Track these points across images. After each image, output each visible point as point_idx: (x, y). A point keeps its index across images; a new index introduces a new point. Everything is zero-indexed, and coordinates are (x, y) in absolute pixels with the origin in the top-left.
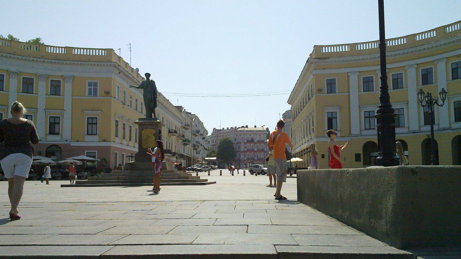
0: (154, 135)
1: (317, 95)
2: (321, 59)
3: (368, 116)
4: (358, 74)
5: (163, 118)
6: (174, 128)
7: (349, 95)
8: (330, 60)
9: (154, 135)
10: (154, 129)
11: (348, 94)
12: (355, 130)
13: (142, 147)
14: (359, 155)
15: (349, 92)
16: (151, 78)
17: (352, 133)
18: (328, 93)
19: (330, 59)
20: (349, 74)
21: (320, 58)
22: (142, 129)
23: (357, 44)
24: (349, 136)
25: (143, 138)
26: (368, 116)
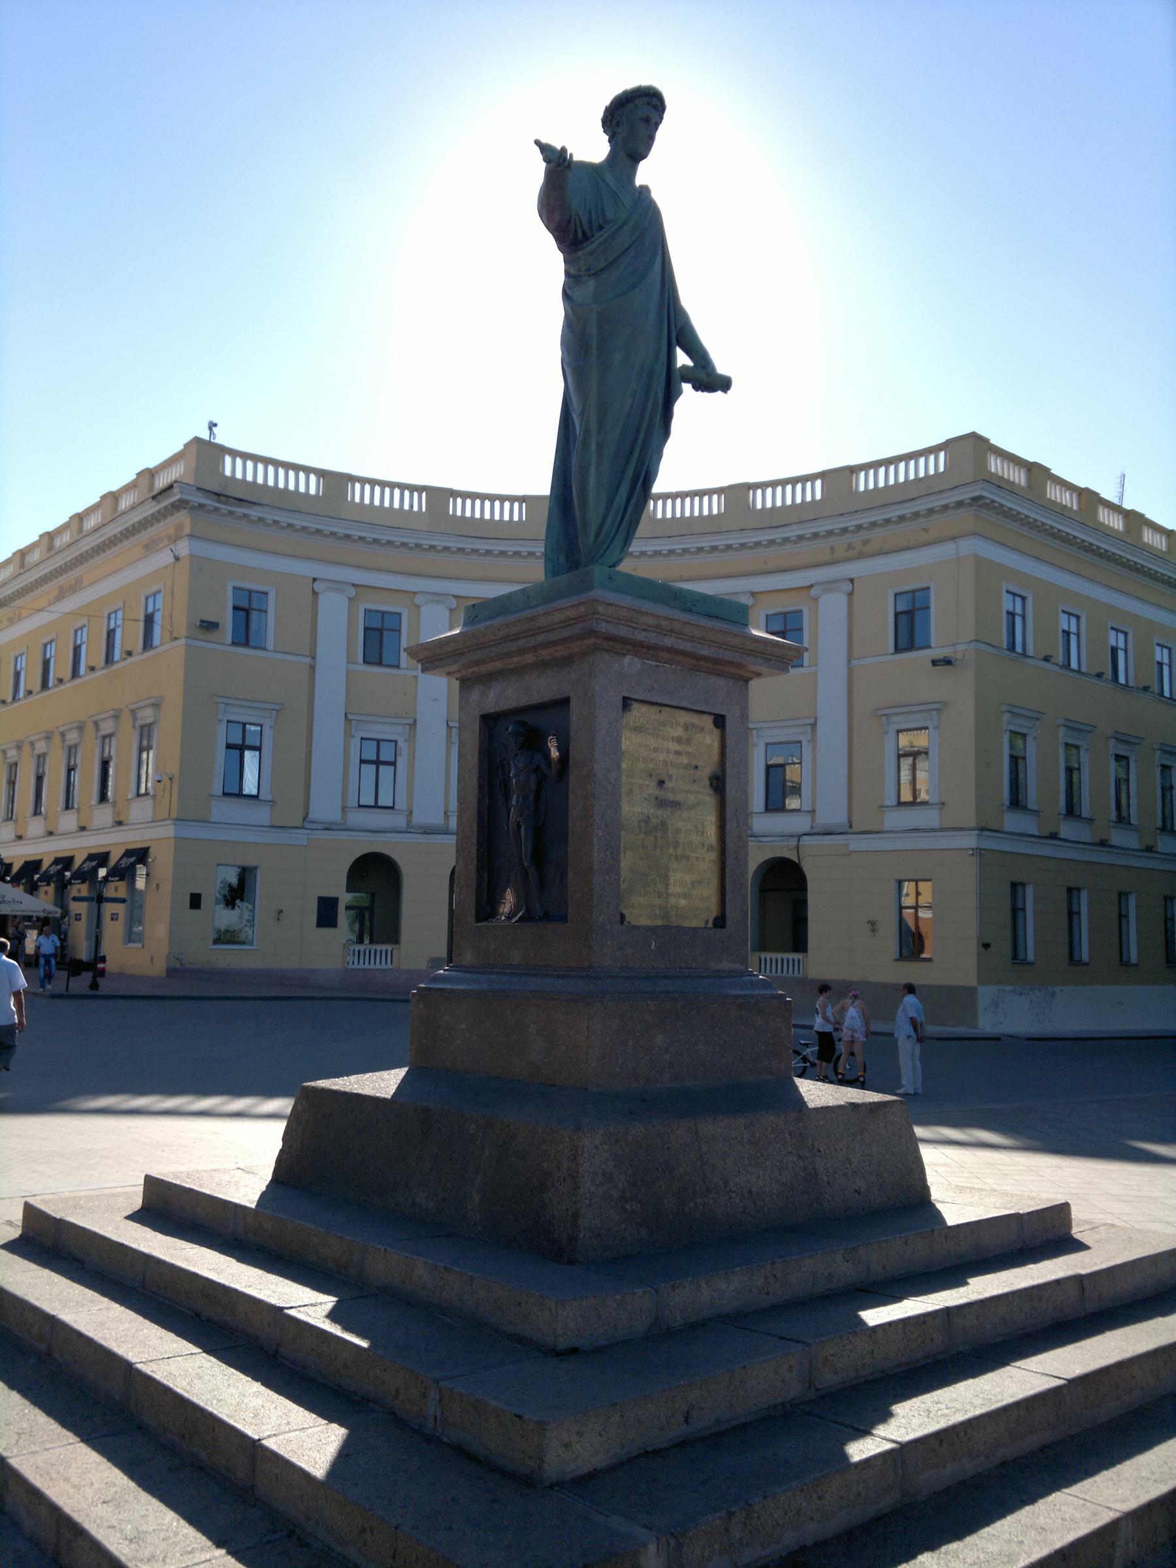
0: (718, 783)
1: (196, 643)
2: (222, 498)
3: (374, 758)
4: (352, 592)
7: (313, 668)
8: (254, 512)
10: (720, 721)
11: (308, 660)
12: (325, 807)
13: (623, 917)
14: (334, 901)
15: (314, 658)
16: (646, 174)
17: (311, 816)
18: (234, 644)
19: (257, 508)
20: (317, 587)
21: (218, 495)
22: (626, 703)
23: (352, 479)
24: (303, 828)
25: (626, 808)
26: (374, 758)
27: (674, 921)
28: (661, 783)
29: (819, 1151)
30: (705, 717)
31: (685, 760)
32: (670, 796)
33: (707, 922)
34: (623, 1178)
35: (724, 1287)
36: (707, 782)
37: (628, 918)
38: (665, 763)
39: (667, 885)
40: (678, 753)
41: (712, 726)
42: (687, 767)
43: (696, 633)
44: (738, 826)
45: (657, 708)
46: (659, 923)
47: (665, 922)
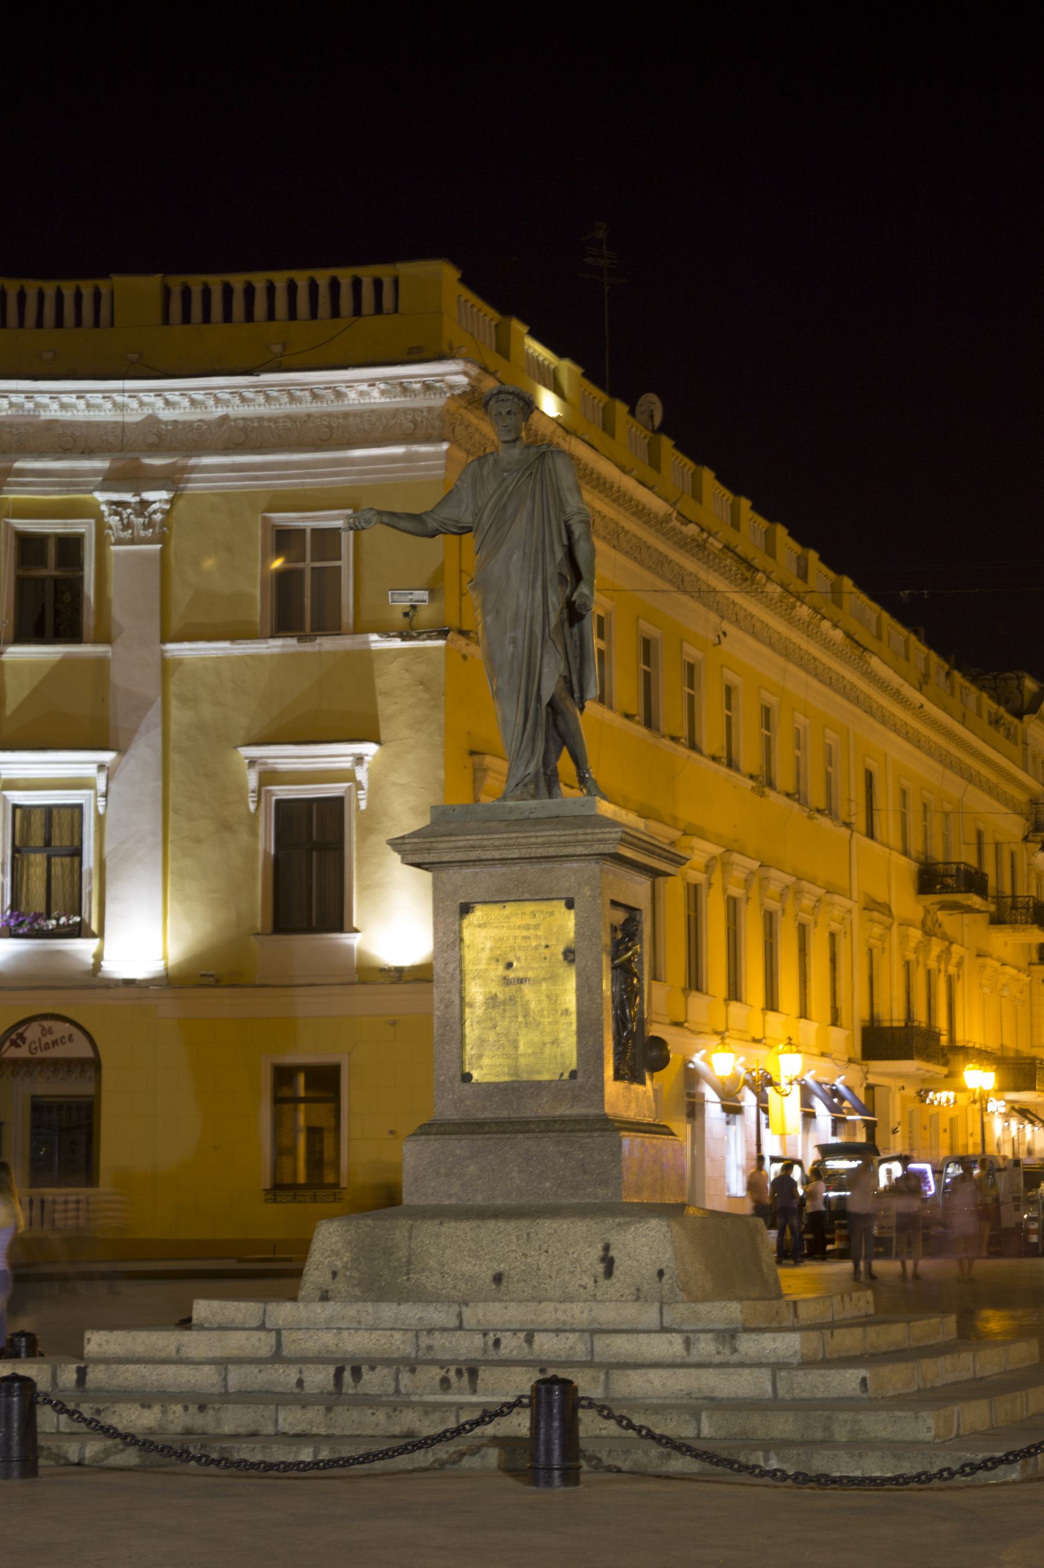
5: (869, 776)
6: (967, 856)
9: (569, 955)
10: (570, 904)
13: (467, 1078)
22: (466, 909)
27: (525, 1077)
28: (509, 965)
29: (547, 1252)
30: (555, 902)
31: (534, 944)
32: (521, 975)
33: (562, 1075)
34: (348, 1254)
35: (319, 1311)
36: (561, 957)
37: (476, 1075)
38: (513, 949)
39: (516, 1048)
40: (526, 938)
41: (564, 909)
42: (536, 948)
43: (496, 843)
44: (590, 991)
45: (501, 905)
46: (507, 1079)
47: (514, 1078)
